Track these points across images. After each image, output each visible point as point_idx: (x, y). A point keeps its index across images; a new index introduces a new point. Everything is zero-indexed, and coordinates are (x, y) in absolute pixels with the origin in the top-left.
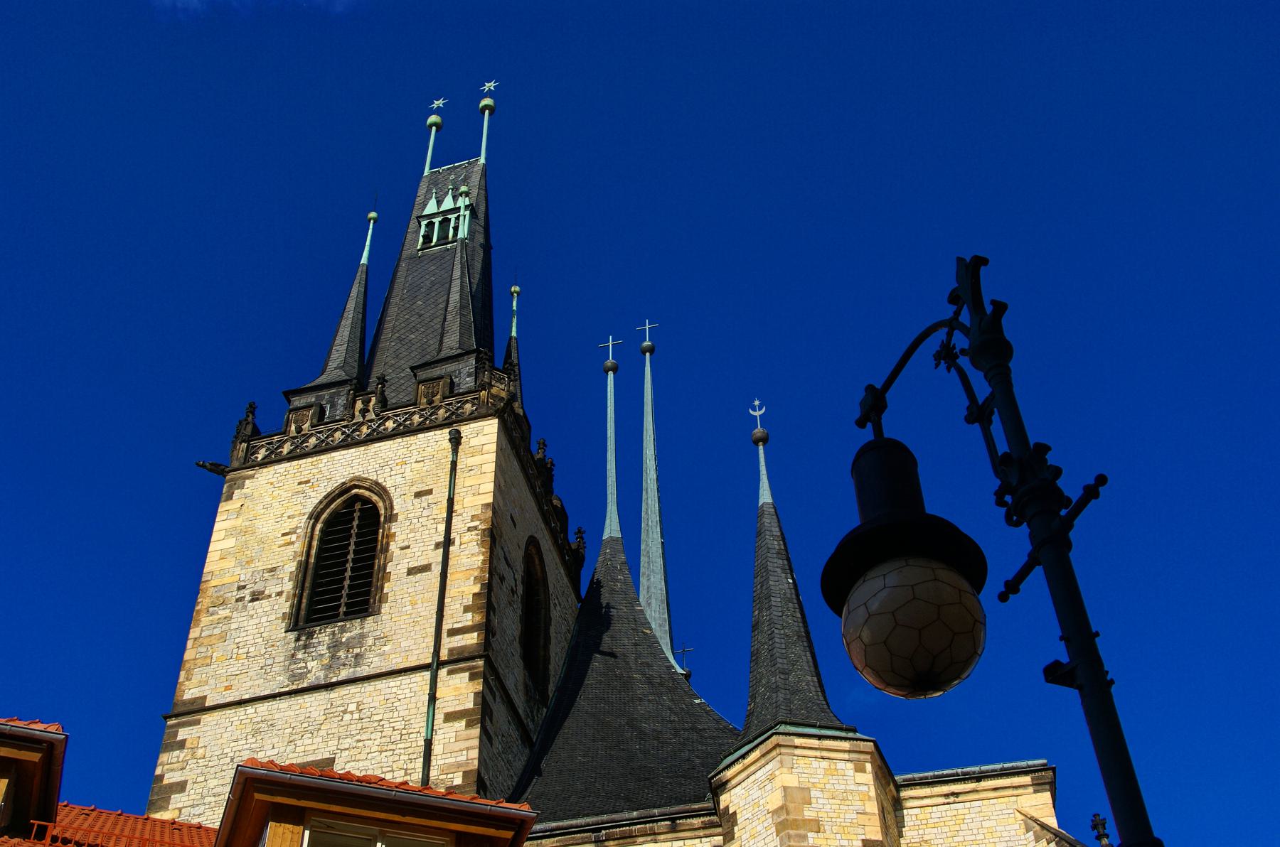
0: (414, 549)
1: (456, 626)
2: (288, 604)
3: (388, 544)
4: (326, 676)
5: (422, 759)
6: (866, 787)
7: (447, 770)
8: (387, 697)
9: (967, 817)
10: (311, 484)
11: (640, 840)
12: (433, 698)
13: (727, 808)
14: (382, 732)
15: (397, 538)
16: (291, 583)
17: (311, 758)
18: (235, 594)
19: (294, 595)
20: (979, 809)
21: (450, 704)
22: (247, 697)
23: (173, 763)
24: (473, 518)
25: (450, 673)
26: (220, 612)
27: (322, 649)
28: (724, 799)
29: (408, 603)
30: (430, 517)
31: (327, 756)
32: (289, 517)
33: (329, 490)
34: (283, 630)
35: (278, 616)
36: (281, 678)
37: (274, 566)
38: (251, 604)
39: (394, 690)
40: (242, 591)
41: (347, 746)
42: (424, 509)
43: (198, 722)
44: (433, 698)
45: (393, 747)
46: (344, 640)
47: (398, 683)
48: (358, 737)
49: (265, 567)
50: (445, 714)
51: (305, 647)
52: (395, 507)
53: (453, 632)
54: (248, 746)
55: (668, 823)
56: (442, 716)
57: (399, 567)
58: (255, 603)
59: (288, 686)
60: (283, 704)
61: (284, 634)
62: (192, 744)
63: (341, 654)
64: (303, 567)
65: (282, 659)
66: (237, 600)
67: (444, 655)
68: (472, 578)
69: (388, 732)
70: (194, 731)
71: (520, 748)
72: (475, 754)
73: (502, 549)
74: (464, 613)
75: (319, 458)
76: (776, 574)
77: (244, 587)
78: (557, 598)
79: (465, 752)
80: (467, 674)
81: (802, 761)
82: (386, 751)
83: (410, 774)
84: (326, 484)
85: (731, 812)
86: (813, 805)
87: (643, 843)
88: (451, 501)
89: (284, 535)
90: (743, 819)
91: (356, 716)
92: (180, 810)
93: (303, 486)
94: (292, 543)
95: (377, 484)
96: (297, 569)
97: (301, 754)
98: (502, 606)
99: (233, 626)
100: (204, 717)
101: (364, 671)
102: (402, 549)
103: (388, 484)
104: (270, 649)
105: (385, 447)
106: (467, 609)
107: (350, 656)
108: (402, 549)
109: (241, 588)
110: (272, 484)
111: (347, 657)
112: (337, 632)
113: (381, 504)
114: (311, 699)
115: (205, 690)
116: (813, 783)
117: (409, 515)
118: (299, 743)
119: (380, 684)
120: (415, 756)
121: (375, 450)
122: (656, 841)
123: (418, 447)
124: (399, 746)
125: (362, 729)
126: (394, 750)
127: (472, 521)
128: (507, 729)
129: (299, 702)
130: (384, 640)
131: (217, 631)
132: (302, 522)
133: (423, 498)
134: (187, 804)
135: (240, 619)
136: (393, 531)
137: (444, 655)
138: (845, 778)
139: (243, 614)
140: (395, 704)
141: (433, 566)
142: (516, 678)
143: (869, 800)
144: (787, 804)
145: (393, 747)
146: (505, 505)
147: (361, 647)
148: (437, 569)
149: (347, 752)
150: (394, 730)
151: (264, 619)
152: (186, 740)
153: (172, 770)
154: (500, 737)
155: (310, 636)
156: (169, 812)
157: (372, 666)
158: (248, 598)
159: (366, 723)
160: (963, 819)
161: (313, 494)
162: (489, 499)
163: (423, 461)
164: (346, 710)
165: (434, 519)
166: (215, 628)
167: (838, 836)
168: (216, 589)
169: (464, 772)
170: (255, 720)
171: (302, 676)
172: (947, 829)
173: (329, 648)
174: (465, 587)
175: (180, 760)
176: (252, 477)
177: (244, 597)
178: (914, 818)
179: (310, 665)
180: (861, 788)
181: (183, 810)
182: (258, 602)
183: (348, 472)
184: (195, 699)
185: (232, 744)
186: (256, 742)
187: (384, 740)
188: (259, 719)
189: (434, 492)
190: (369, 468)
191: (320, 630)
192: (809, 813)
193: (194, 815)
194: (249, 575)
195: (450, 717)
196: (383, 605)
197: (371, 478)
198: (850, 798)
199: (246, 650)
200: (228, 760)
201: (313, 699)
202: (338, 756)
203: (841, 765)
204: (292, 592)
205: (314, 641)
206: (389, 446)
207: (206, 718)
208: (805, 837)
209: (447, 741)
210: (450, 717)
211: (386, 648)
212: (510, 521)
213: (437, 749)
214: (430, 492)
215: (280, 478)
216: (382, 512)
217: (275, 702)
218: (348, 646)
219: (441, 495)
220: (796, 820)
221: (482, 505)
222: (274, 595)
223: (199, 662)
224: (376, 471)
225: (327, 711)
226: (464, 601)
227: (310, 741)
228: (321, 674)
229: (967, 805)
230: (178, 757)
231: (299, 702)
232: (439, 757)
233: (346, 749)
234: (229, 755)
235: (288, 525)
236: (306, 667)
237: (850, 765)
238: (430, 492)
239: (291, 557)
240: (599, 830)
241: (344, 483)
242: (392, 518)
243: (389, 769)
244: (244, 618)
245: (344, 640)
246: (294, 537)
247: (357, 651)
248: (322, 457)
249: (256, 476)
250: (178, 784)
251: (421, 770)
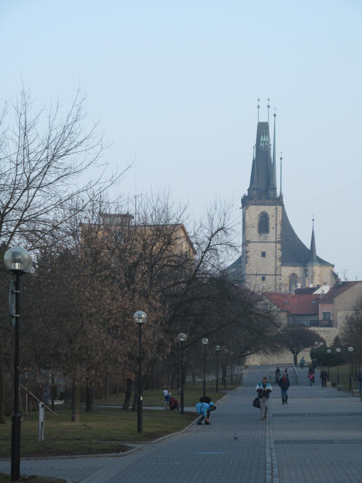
12: (276, 247)
24: (280, 222)
44: (276, 247)
60: (259, 243)
72: (281, 254)
101: (268, 241)
106: (279, 235)
109: (251, 225)
132: (257, 216)
162: (281, 219)
171: (261, 240)
174: (279, 232)
192: (315, 272)
195: (278, 249)
210: (278, 249)
213: (277, 253)
218: (266, 237)
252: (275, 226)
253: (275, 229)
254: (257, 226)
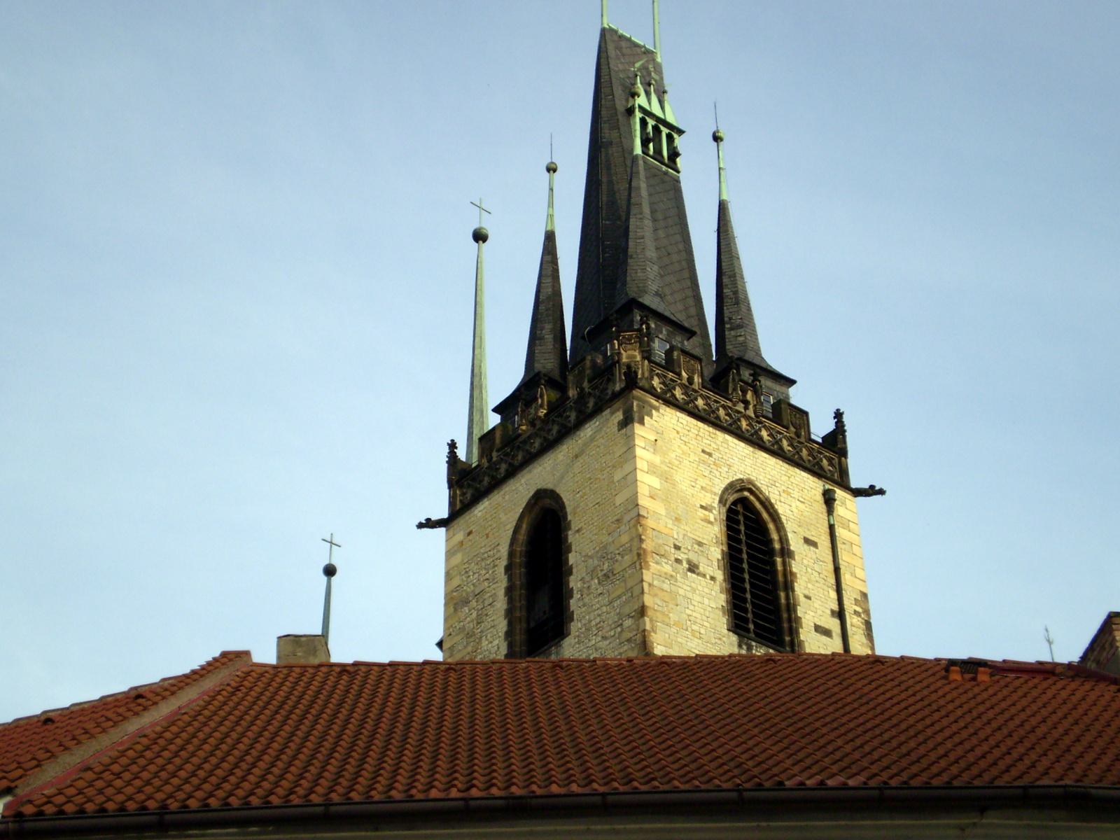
0: (816, 604)
49: (693, 537)
61: (726, 632)
75: (714, 431)
109: (677, 548)
110: (678, 432)
176: (657, 409)
190: (761, 478)
248: (719, 433)
252: (834, 625)
254: (720, 576)
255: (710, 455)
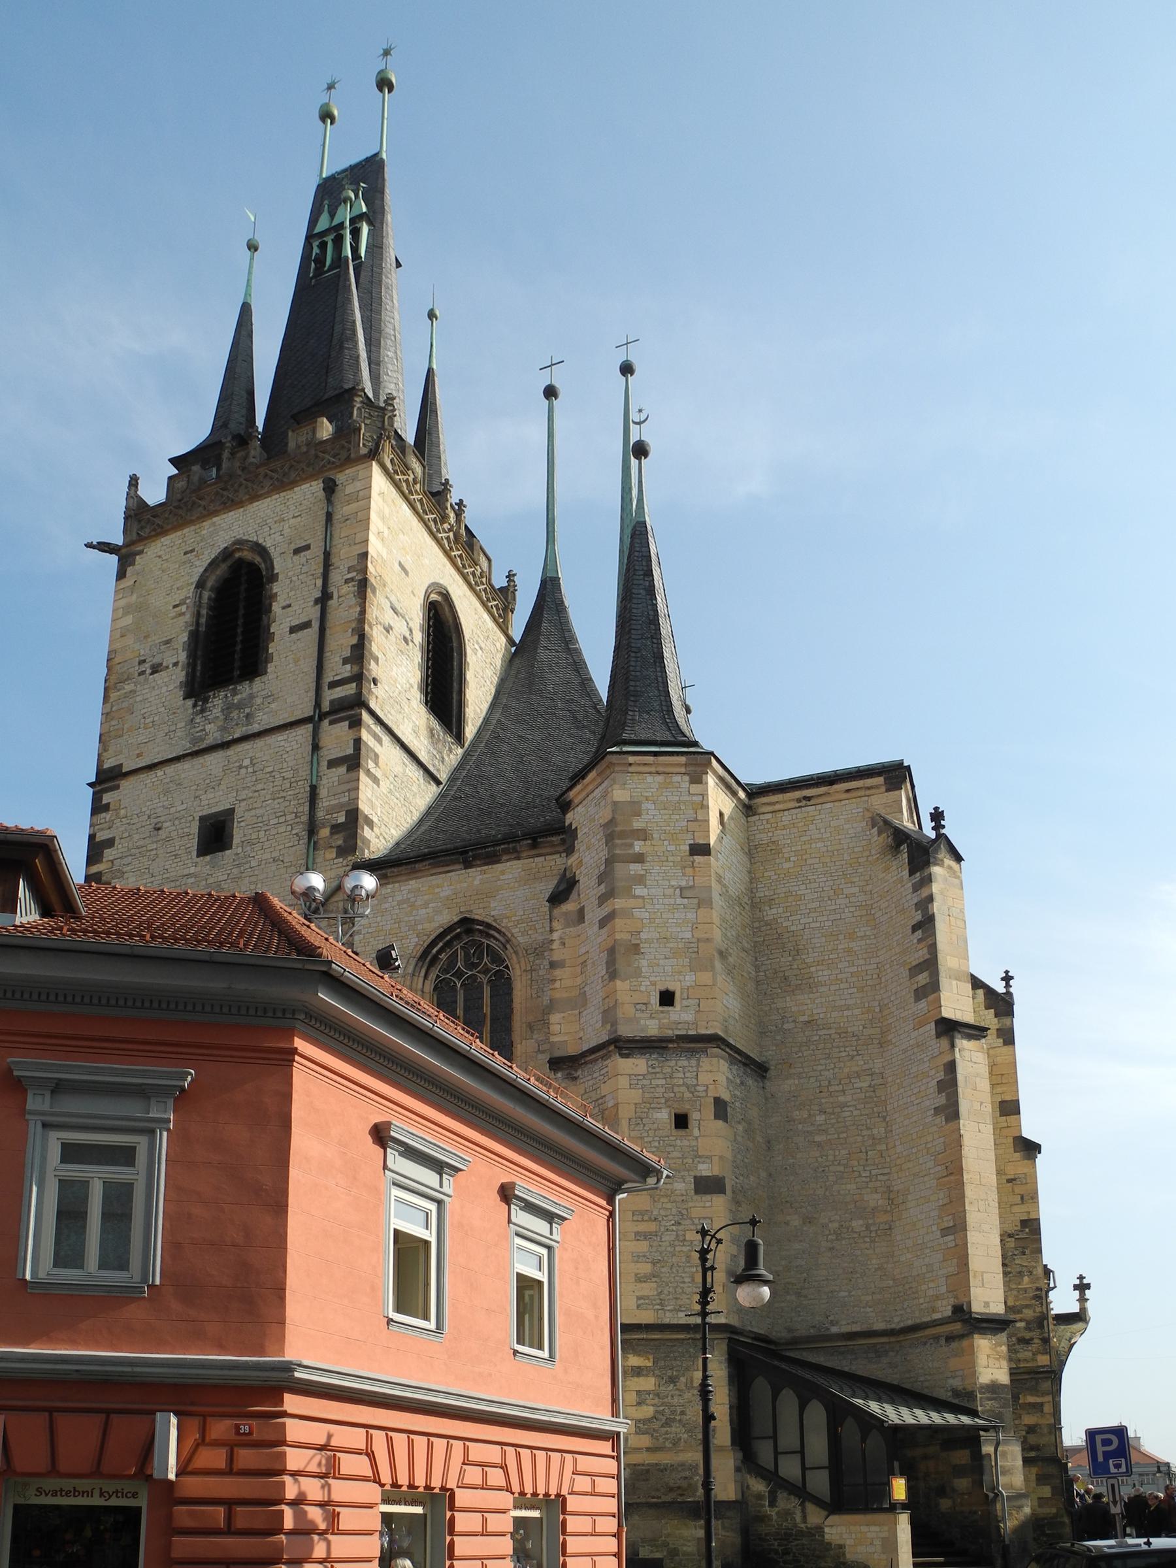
0: (295, 607)
1: (336, 678)
2: (184, 673)
3: (271, 605)
4: (222, 736)
5: (308, 803)
6: (701, 797)
7: (332, 810)
8: (277, 750)
9: (816, 818)
10: (195, 553)
11: (505, 857)
12: (316, 747)
13: (571, 824)
14: (273, 782)
15: (278, 598)
16: (185, 652)
17: (214, 810)
18: (137, 669)
19: (188, 664)
20: (830, 810)
21: (332, 751)
22: (156, 761)
23: (101, 824)
25: (331, 723)
26: (126, 687)
27: (217, 712)
28: (569, 818)
29: (291, 661)
30: (309, 573)
31: (228, 806)
32: (178, 589)
33: (213, 556)
34: (181, 698)
35: (175, 685)
36: (183, 742)
37: (169, 638)
38: (152, 676)
39: (282, 743)
40: (141, 666)
41: (244, 797)
42: (303, 565)
43: (117, 787)
44: (316, 747)
45: (284, 794)
46: (235, 701)
47: (285, 737)
48: (254, 788)
49: (160, 641)
50: (328, 761)
51: (202, 711)
52: (275, 566)
53: (333, 685)
54: (161, 804)
55: (529, 842)
56: (326, 763)
57: (282, 627)
58: (155, 675)
59: (190, 748)
60: (186, 765)
62: (115, 806)
63: (235, 714)
64: (194, 636)
65: (183, 724)
66: (140, 674)
67: (326, 706)
68: (350, 630)
69: (278, 782)
70: (115, 795)
71: (422, 786)
73: (387, 598)
74: (343, 665)
76: (640, 596)
77: (144, 661)
78: (478, 643)
79: (347, 794)
80: (347, 723)
81: (636, 777)
82: (278, 798)
83: (300, 817)
84: (209, 551)
85: (573, 828)
86: (643, 817)
87: (507, 861)
88: (327, 555)
89: (175, 607)
90: (582, 833)
91: (250, 770)
92: (112, 861)
93: (189, 555)
94: (183, 614)
95: (257, 544)
96: (189, 638)
97: (206, 807)
98: (389, 655)
99: (139, 699)
100: (123, 782)
101: (256, 728)
102: (284, 608)
103: (268, 544)
104: (171, 717)
105: (263, 506)
106: (345, 661)
107: (242, 715)
108: (284, 608)
110: (160, 557)
111: (239, 717)
112: (229, 695)
113: (263, 566)
114: (210, 759)
115: (120, 759)
116: (646, 797)
117: (290, 574)
118: (203, 797)
119: (272, 740)
120: (303, 801)
121: (254, 509)
122: (518, 858)
123: (294, 501)
124: (289, 793)
125: (256, 781)
126: (285, 797)
127: (348, 573)
128: (402, 770)
129: (201, 761)
130: (271, 697)
131: (125, 705)
133: (302, 554)
134: (116, 856)
135: (144, 692)
136: (274, 591)
137: (326, 706)
138: (679, 790)
139: (145, 687)
140: (284, 756)
141: (313, 623)
142: (413, 722)
143: (701, 808)
144: (616, 816)
145: (284, 794)
146: (390, 552)
147: (251, 707)
148: (316, 625)
149: (245, 802)
150: (284, 780)
151: (164, 689)
152: (109, 803)
153: (102, 829)
154: (391, 779)
155: (206, 700)
156: (103, 864)
157: (263, 723)
158: (149, 671)
159: (260, 775)
160: (812, 821)
161: (197, 563)
163: (300, 515)
164: (241, 765)
165: (313, 575)
166: (123, 702)
167: (666, 843)
168: (120, 665)
169: (347, 812)
170: (166, 781)
171: (202, 739)
172: (795, 830)
173: (223, 711)
175: (107, 820)
177: (145, 671)
178: (765, 823)
179: (208, 727)
180: (695, 798)
181: (115, 862)
182: (157, 674)
183: (229, 537)
184: (115, 766)
185: (148, 803)
186: (167, 800)
187: (276, 789)
188: (168, 780)
189: (312, 547)
191: (214, 694)
192: (637, 824)
193: (124, 865)
194: (147, 651)
195: (333, 764)
196: (269, 665)
197: (251, 539)
198: (683, 808)
199: (151, 719)
200: (146, 817)
201: (212, 758)
202: (237, 806)
203: (677, 778)
204: (186, 662)
205: (208, 705)
206: (266, 504)
207: (125, 784)
208: (631, 845)
209: (331, 784)
211: (273, 706)
212: (397, 568)
213: (323, 792)
214: (307, 547)
215: (168, 550)
216: (264, 573)
217: (179, 764)
218: (239, 707)
219: (317, 550)
220: (622, 831)
221: (358, 555)
222: (171, 666)
223: (113, 734)
224: (256, 532)
225: (225, 768)
226: (343, 653)
227: (212, 795)
228: (218, 735)
229: (819, 807)
230: (105, 818)
231: (201, 761)
232: (324, 800)
233: (245, 800)
234: (146, 813)
235: (177, 597)
236: (204, 730)
237: (687, 778)
238: (307, 547)
239: (183, 628)
240: (467, 852)
241: (226, 548)
242: (273, 578)
243: (282, 814)
244: (147, 691)
245: (235, 701)
246: (184, 608)
247: (247, 710)
249: (145, 551)
250: (108, 840)
251: (308, 812)
253: (312, 633)
255: (192, 551)
